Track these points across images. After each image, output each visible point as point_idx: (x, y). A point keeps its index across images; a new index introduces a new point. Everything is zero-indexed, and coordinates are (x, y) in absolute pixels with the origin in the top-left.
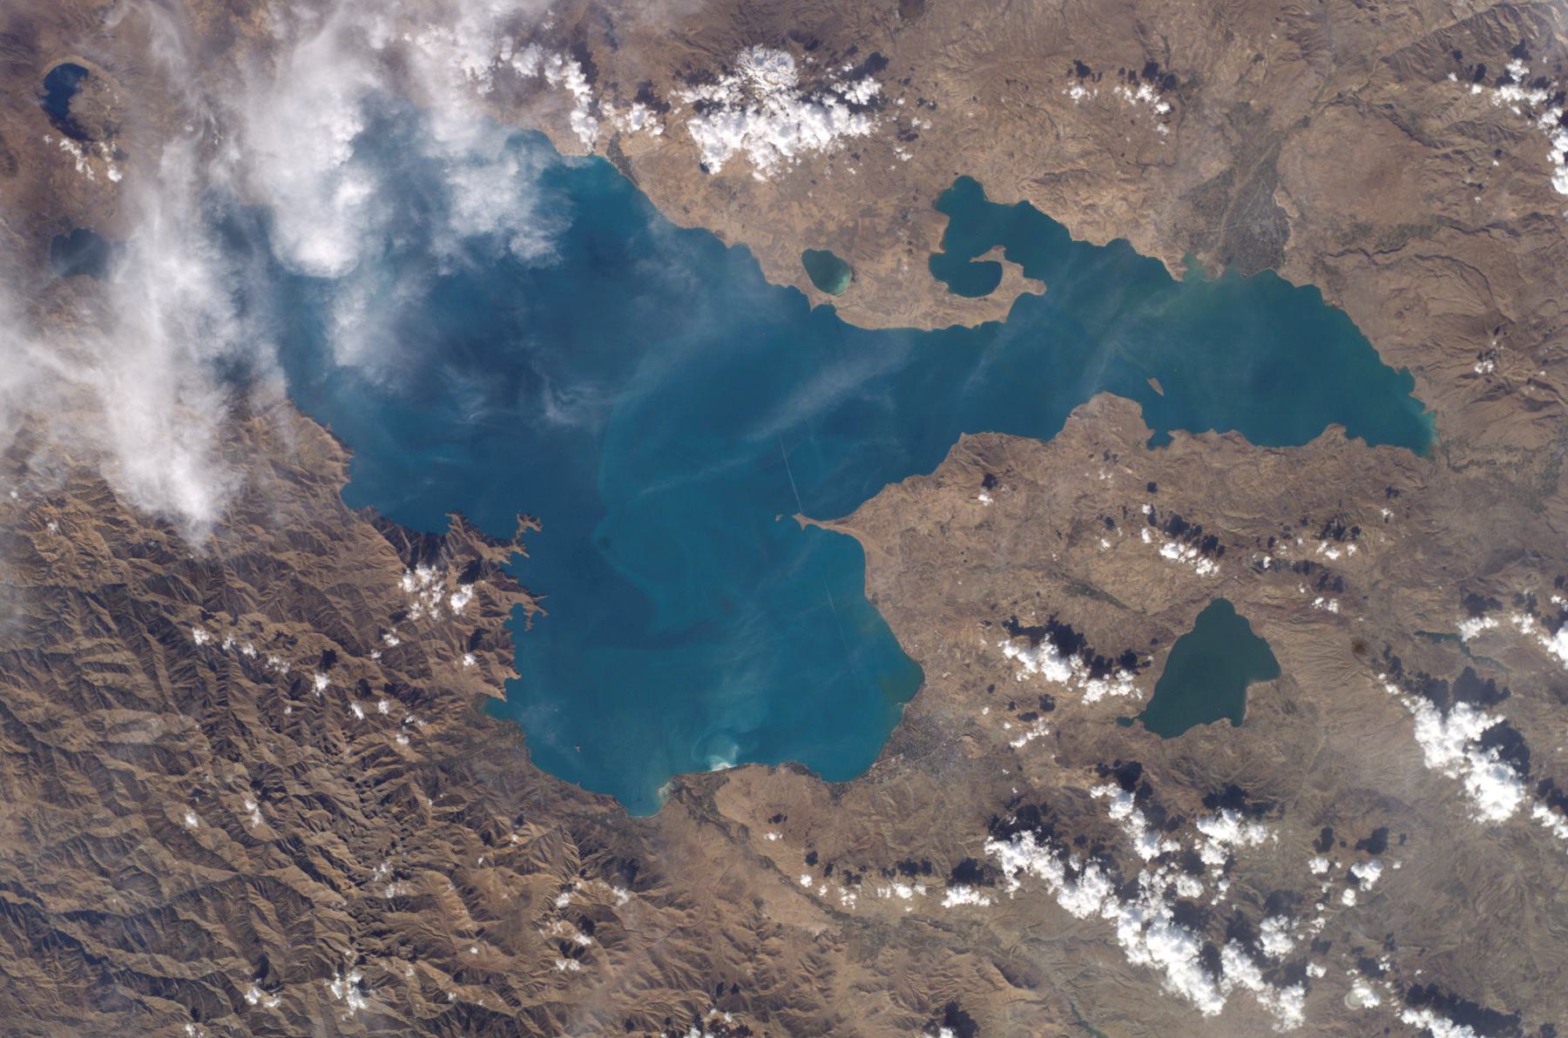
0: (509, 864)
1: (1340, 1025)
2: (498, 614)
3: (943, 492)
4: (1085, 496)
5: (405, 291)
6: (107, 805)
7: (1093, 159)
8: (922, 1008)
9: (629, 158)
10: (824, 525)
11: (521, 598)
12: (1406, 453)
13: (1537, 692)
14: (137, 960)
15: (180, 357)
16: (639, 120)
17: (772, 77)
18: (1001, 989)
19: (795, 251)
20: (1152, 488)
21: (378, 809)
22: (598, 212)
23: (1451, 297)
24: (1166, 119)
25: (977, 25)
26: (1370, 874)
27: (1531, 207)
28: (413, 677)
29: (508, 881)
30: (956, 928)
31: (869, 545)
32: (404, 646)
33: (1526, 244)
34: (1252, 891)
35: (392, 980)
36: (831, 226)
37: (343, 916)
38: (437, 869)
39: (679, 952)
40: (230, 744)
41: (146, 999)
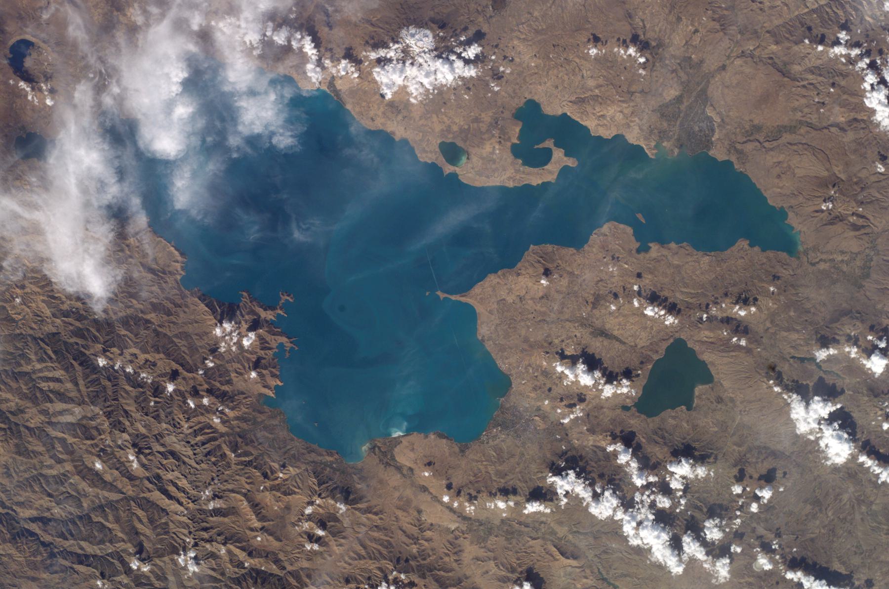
0: (278, 490)
1: (751, 580)
2: (270, 349)
3: (520, 278)
4: (601, 280)
5: (213, 167)
6: (51, 457)
7: (603, 89)
8: (513, 570)
9: (340, 90)
10: (453, 298)
11: (283, 340)
12: (783, 255)
13: (860, 390)
14: (69, 544)
15: (87, 205)
16: (345, 69)
17: (420, 44)
18: (557, 560)
19: (435, 142)
20: (639, 275)
21: (204, 459)
22: (322, 121)
23: (808, 166)
24: (644, 66)
25: (536, 14)
26: (766, 494)
27: (853, 115)
28: (222, 384)
29: (278, 500)
30: (531, 525)
31: (479, 309)
32: (217, 367)
33: (850, 136)
34: (699, 504)
35: (213, 556)
36: (455, 128)
37: (185, 519)
38: (237, 493)
39: (375, 539)
40: (120, 422)
41: (75, 566)
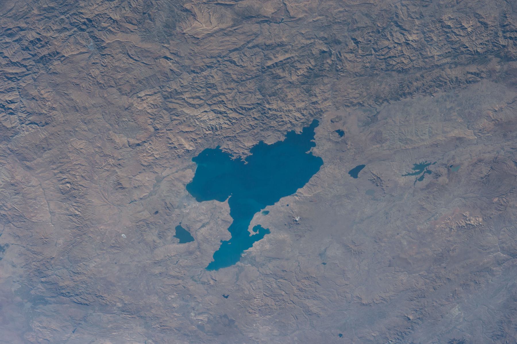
31: (222, 203)
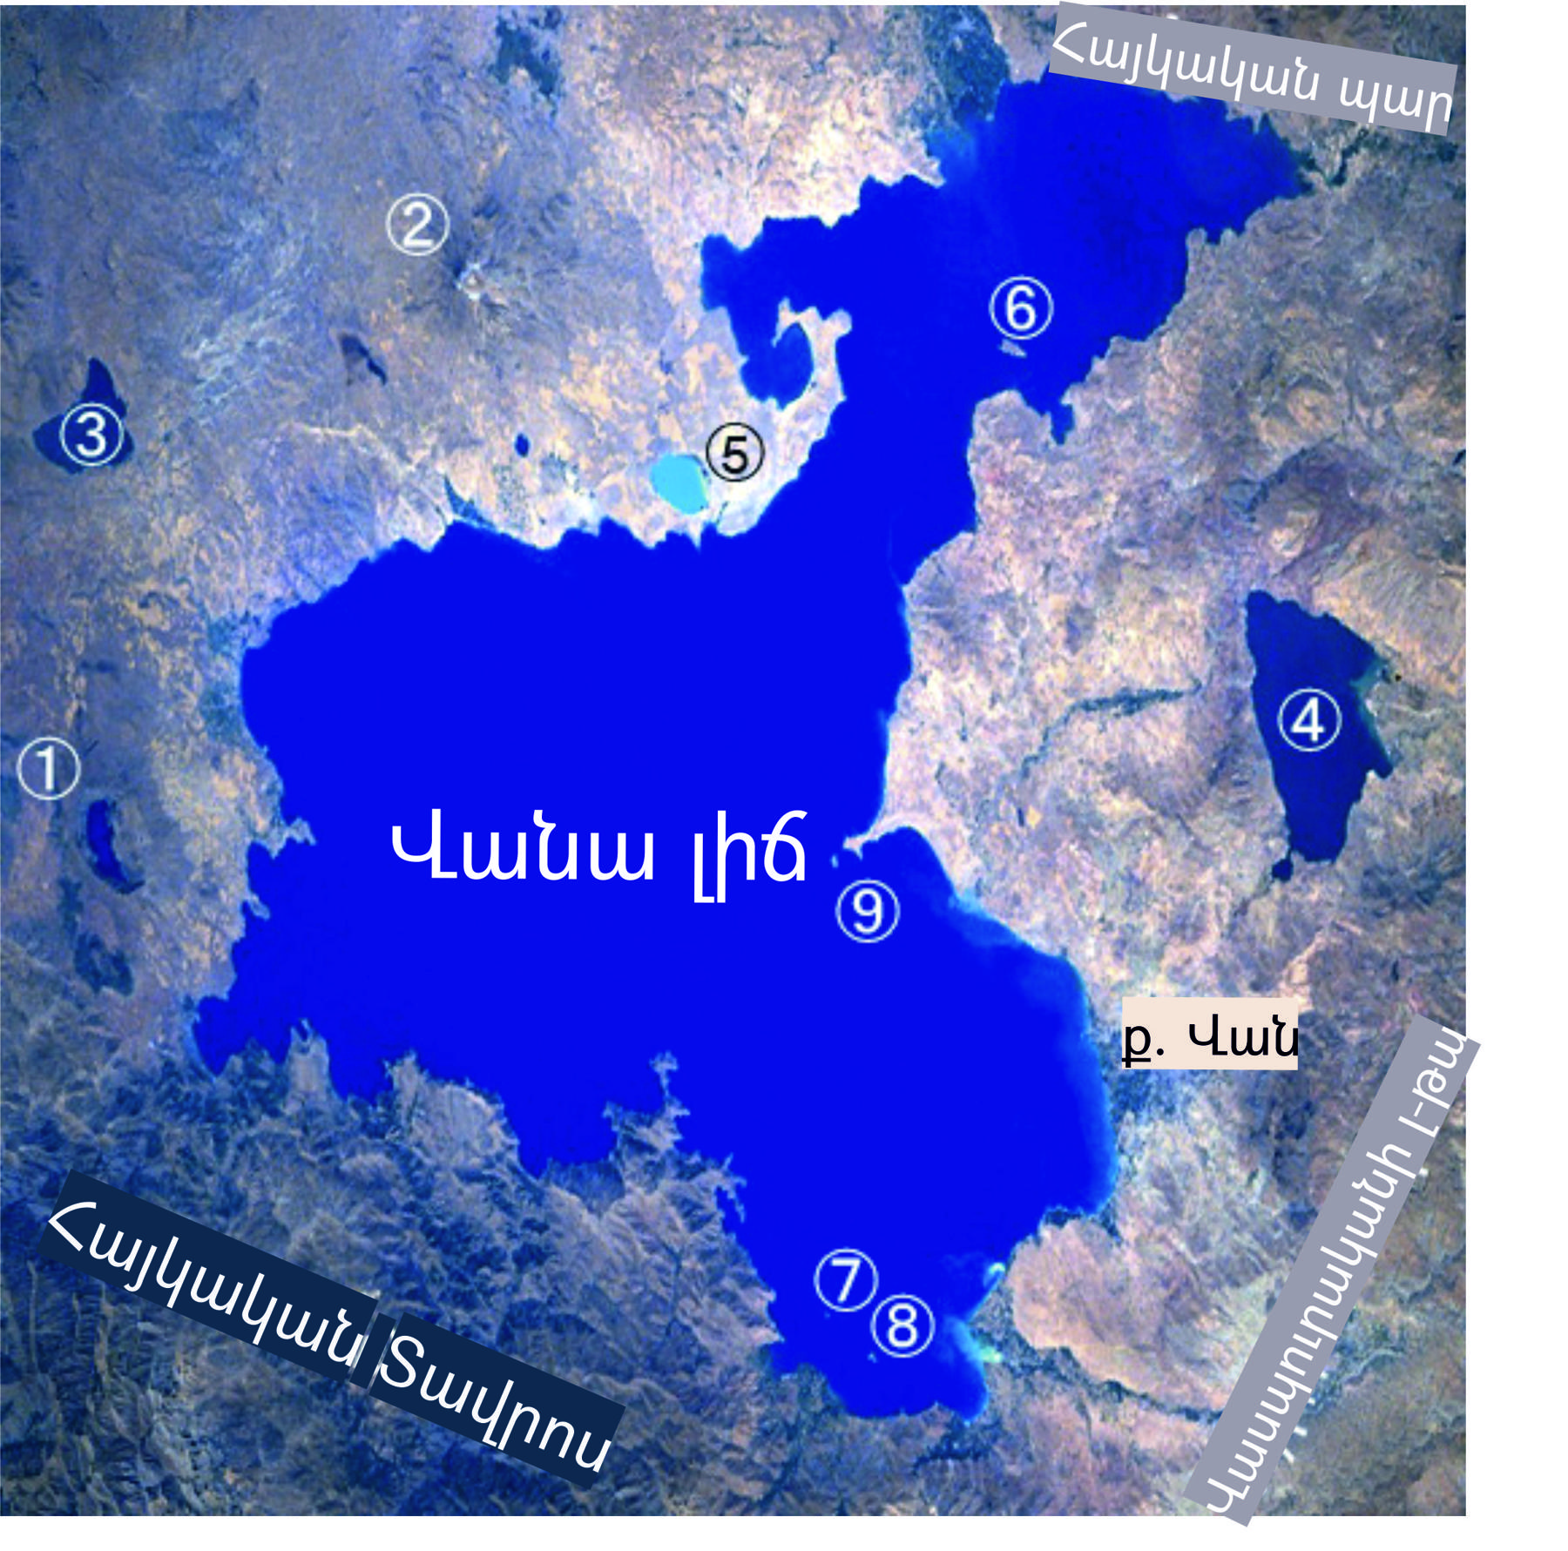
10: (876, 831)
31: (924, 827)
